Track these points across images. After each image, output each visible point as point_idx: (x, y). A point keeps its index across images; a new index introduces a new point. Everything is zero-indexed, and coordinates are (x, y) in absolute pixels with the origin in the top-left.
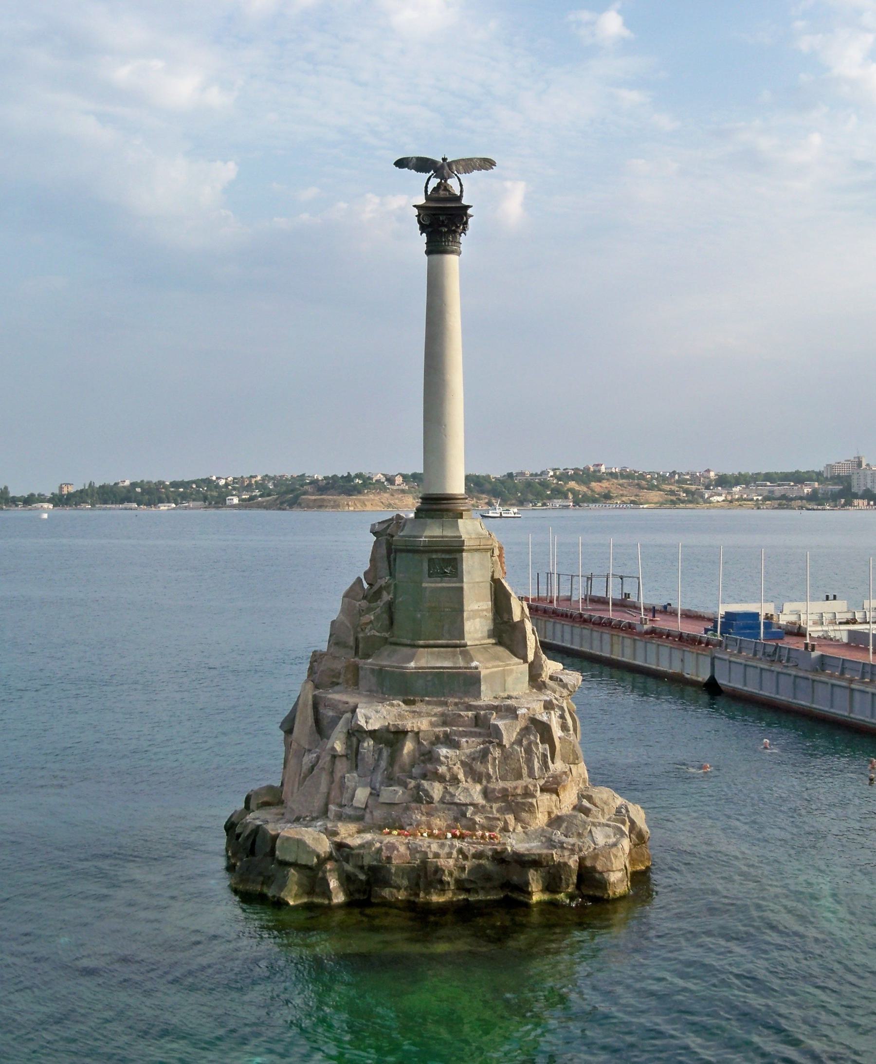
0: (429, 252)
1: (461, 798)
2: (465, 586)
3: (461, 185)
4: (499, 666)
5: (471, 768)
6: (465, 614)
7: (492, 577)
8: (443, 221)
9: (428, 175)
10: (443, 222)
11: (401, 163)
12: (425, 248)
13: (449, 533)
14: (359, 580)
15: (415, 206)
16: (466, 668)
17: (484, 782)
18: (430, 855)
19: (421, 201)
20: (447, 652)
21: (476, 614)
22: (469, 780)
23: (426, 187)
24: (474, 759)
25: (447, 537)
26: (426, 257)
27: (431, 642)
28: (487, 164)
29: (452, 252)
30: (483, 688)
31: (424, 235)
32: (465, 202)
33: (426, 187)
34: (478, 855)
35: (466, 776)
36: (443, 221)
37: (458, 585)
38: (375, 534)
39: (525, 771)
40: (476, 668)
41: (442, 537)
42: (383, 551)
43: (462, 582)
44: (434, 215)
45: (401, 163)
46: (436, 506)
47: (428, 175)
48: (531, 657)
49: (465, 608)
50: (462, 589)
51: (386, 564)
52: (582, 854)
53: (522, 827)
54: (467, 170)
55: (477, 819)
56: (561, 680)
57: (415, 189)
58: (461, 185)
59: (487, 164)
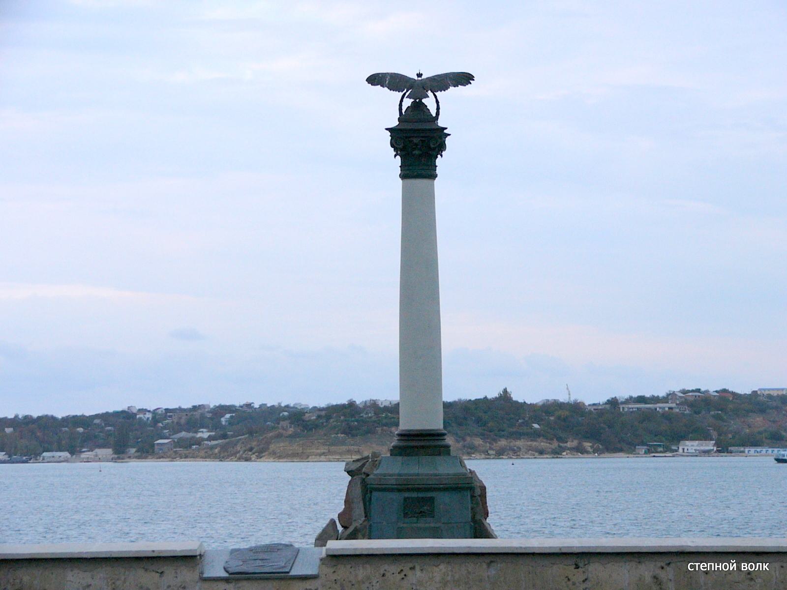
0: (403, 176)
3: (437, 102)
8: (418, 144)
9: (401, 94)
10: (416, 145)
11: (374, 80)
14: (333, 522)
15: (387, 129)
19: (394, 123)
23: (401, 105)
25: (422, 475)
26: (400, 181)
28: (464, 79)
31: (398, 158)
32: (441, 123)
33: (401, 105)
36: (418, 144)
38: (350, 472)
41: (418, 475)
42: (358, 491)
45: (374, 80)
47: (401, 94)
51: (361, 505)
54: (445, 88)
57: (389, 107)
58: (437, 102)
59: (464, 79)
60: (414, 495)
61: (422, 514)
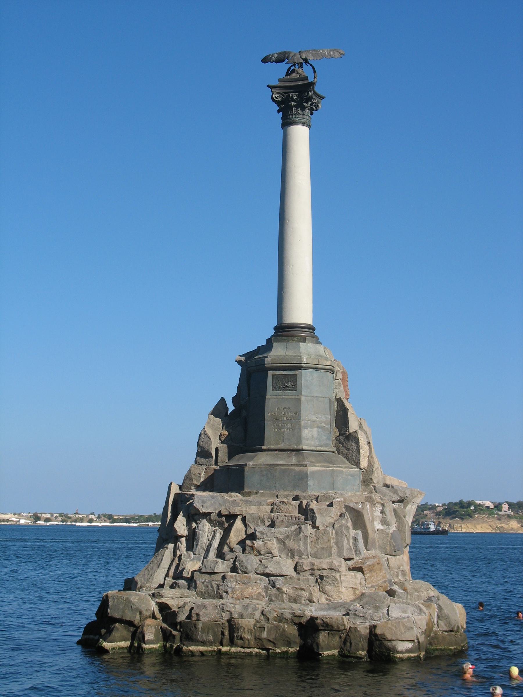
1: (271, 569)
2: (303, 398)
3: (315, 72)
4: (329, 467)
5: (284, 544)
6: (303, 423)
7: (336, 397)
12: (280, 122)
13: (290, 353)
15: (268, 86)
16: (297, 465)
17: (297, 558)
18: (236, 616)
20: (284, 454)
21: (313, 424)
22: (282, 556)
24: (288, 536)
27: (273, 447)
29: (303, 124)
30: (310, 483)
34: (280, 618)
35: (280, 551)
37: (297, 397)
39: (334, 549)
40: (306, 465)
43: (301, 394)
44: (285, 93)
46: (284, 331)
48: (364, 463)
49: (303, 417)
50: (299, 400)
52: (373, 623)
53: (327, 599)
55: (285, 589)
56: (392, 487)
60: (282, 372)
61: (286, 388)
